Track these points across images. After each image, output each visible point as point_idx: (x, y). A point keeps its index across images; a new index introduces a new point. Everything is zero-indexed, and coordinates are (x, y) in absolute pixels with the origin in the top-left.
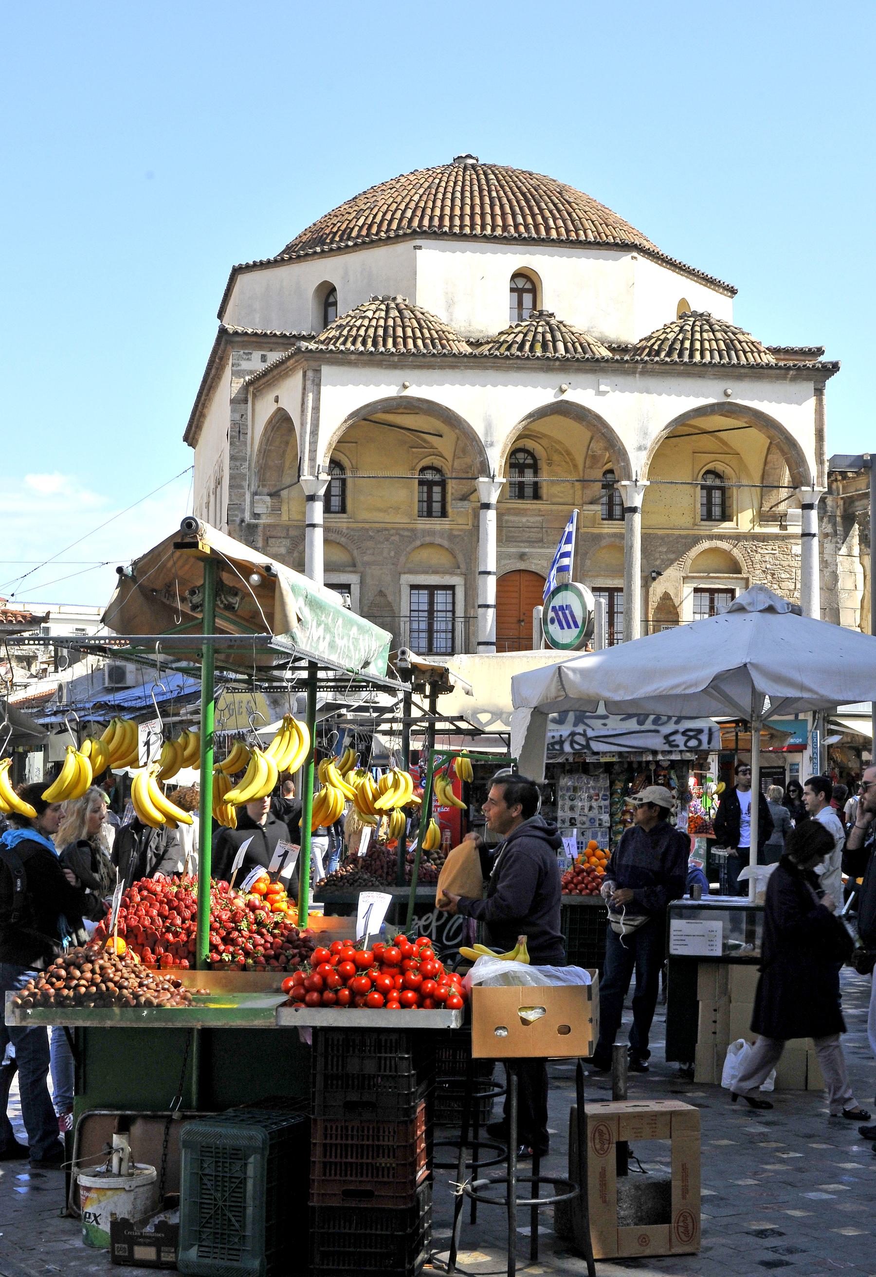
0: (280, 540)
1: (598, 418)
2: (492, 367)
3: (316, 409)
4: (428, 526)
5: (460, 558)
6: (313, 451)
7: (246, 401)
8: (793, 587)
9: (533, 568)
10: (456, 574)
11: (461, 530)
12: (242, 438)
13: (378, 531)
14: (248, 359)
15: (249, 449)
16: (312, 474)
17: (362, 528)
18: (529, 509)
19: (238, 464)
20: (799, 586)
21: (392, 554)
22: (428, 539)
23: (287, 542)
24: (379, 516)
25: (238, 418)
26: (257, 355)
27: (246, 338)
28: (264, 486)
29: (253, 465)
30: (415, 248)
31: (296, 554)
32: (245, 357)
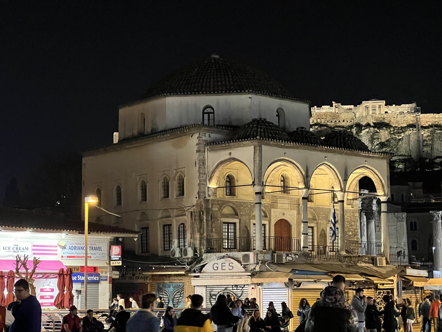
0: (216, 205)
3: (261, 161)
5: (268, 214)
7: (205, 152)
8: (355, 228)
10: (267, 220)
11: (267, 204)
13: (245, 203)
14: (205, 136)
15: (206, 170)
17: (240, 202)
18: (286, 197)
19: (203, 175)
21: (249, 212)
25: (202, 158)
26: (207, 135)
30: (249, 98)
31: (221, 211)
32: (204, 135)
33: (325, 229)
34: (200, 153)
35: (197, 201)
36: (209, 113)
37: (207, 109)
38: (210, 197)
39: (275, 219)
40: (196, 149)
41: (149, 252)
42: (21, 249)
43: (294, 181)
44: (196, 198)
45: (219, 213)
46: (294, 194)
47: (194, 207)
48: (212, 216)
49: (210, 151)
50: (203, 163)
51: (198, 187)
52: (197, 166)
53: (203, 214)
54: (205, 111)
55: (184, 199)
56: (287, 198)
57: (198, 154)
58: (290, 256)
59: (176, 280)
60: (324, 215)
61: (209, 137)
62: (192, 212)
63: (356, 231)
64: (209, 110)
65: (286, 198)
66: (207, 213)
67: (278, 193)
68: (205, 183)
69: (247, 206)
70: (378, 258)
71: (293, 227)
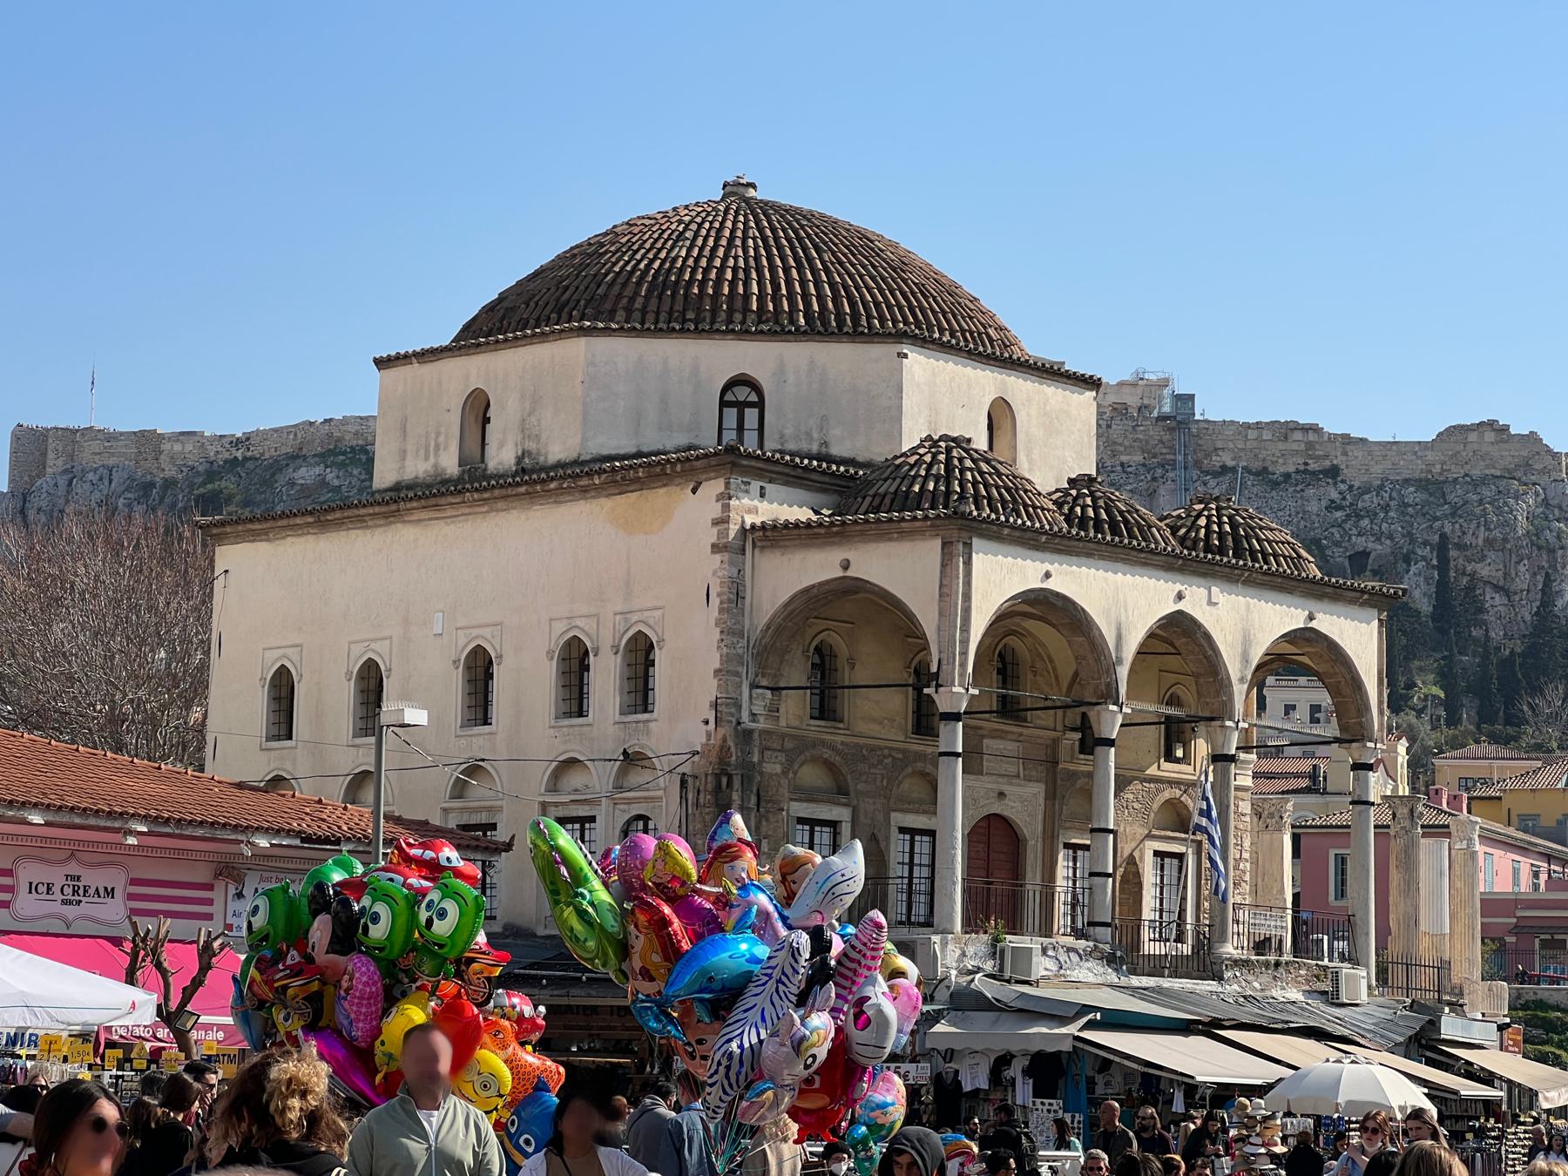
1: (1207, 636)
2: (1122, 559)
3: (967, 597)
4: (922, 748)
6: (964, 653)
9: (1006, 813)
12: (739, 605)
13: (873, 749)
14: (747, 492)
16: (961, 685)
17: (857, 745)
18: (1012, 732)
19: (735, 641)
20: (1246, 855)
21: (885, 783)
22: (919, 765)
23: (782, 757)
24: (874, 729)
25: (736, 575)
26: (756, 485)
27: (753, 463)
28: (763, 676)
29: (751, 646)
31: (791, 775)
32: (743, 487)
33: (1136, 854)
34: (726, 556)
35: (709, 735)
36: (741, 406)
37: (735, 389)
38: (758, 722)
39: (971, 812)
40: (714, 539)
41: (495, 918)
42: (92, 891)
43: (1042, 676)
44: (707, 722)
45: (784, 782)
46: (1039, 722)
47: (696, 758)
48: (762, 794)
49: (763, 548)
50: (739, 596)
51: (716, 681)
52: (715, 601)
53: (729, 784)
54: (729, 397)
55: (652, 725)
56: (1014, 737)
57: (718, 557)
58: (1050, 953)
59: (614, 1028)
60: (1136, 805)
61: (762, 495)
62: (684, 774)
63: (1241, 865)
64: (742, 393)
65: (1009, 737)
66: (746, 780)
67: (987, 716)
68: (740, 669)
69: (880, 762)
70: (1344, 970)
71: (1031, 843)
